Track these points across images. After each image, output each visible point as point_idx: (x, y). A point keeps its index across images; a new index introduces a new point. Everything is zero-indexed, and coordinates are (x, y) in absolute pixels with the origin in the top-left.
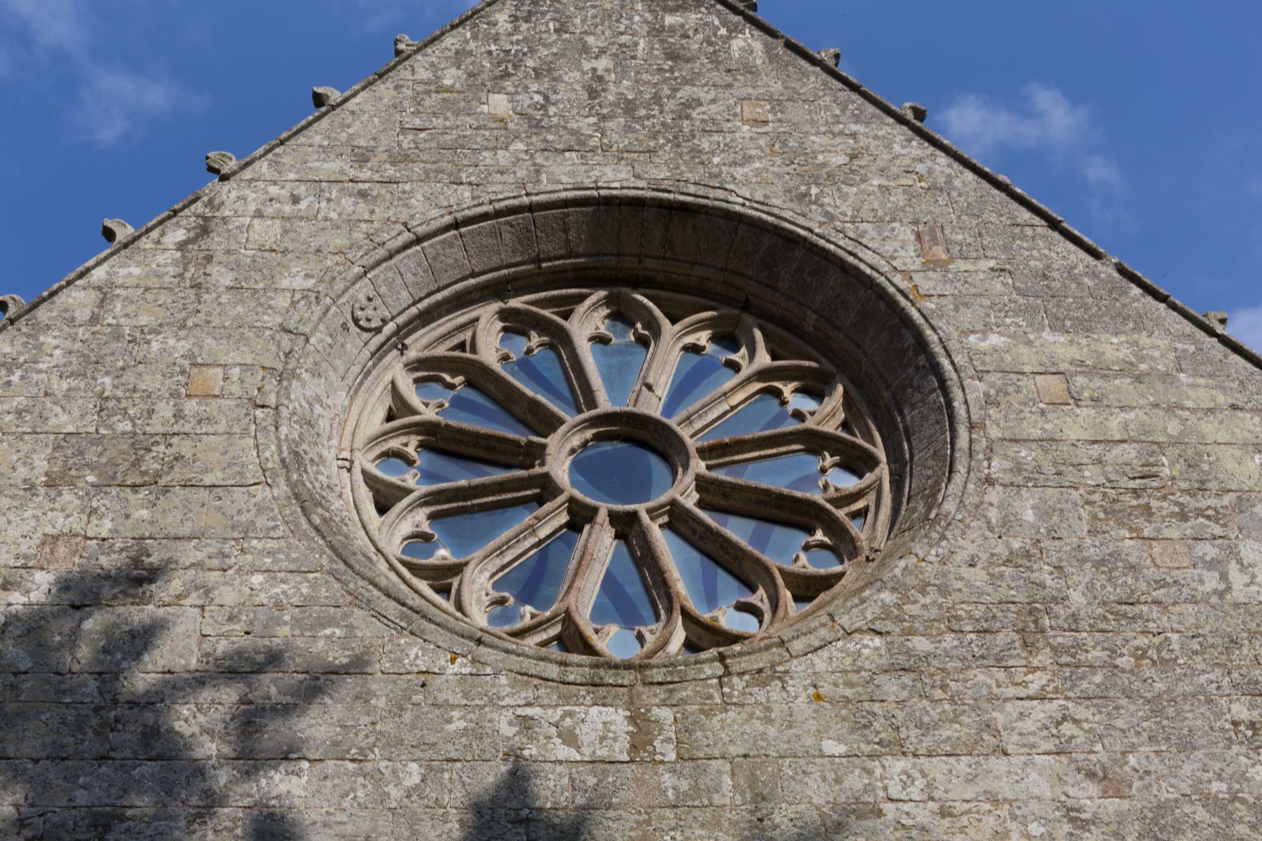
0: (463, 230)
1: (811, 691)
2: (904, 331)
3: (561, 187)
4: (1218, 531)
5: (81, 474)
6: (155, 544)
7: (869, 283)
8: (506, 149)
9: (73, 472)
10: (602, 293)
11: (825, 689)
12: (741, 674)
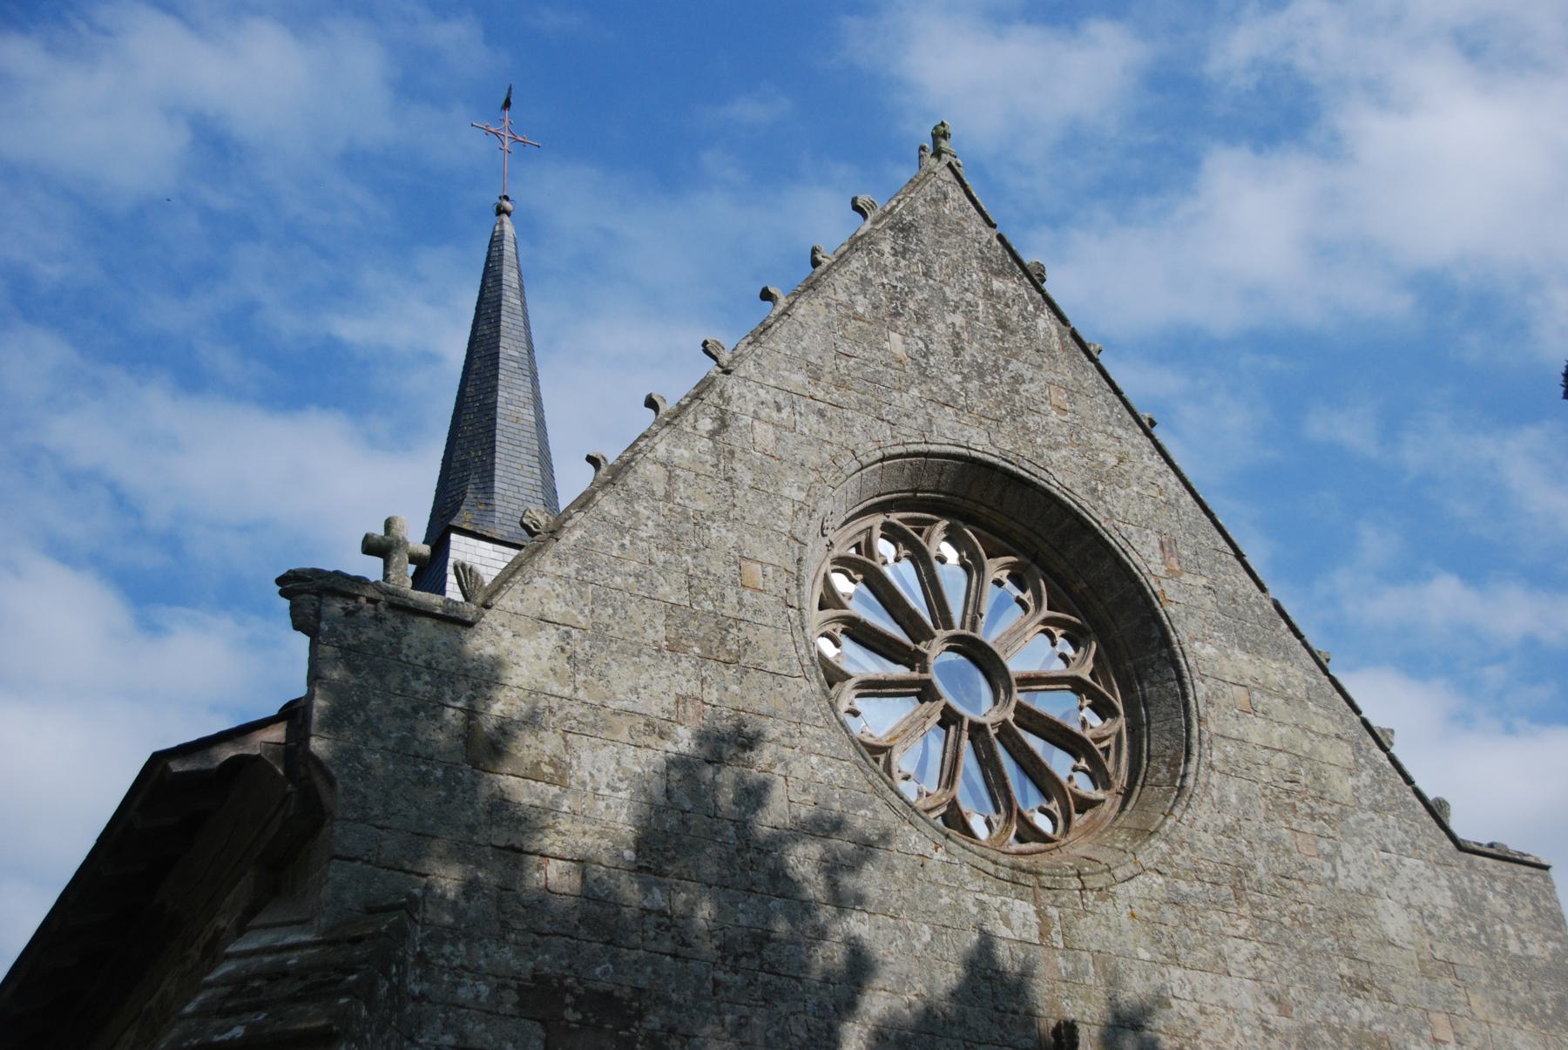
0: (885, 463)
1: (1129, 910)
2: (1153, 624)
3: (946, 441)
4: (1331, 832)
5: (689, 644)
6: (747, 716)
7: (1134, 579)
8: (907, 392)
9: (684, 641)
11: (1136, 911)
12: (1092, 890)
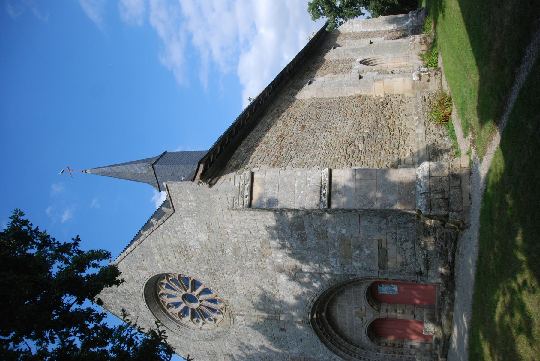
10: (160, 298)
